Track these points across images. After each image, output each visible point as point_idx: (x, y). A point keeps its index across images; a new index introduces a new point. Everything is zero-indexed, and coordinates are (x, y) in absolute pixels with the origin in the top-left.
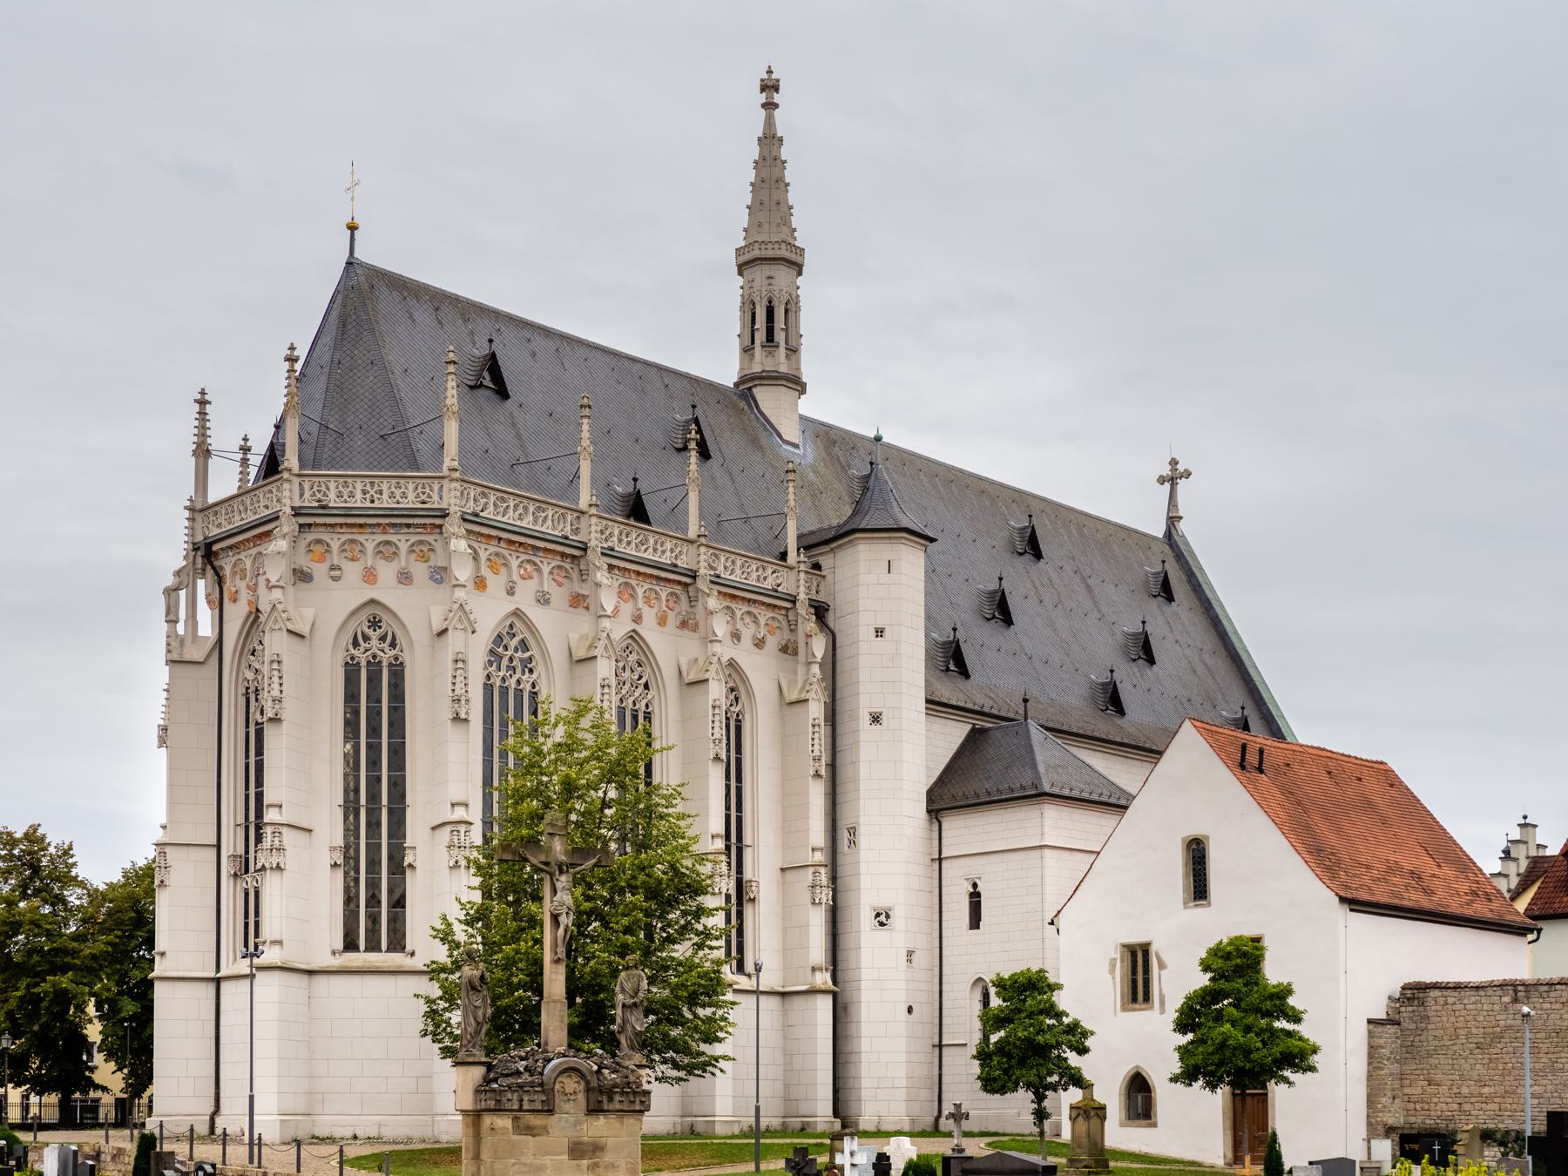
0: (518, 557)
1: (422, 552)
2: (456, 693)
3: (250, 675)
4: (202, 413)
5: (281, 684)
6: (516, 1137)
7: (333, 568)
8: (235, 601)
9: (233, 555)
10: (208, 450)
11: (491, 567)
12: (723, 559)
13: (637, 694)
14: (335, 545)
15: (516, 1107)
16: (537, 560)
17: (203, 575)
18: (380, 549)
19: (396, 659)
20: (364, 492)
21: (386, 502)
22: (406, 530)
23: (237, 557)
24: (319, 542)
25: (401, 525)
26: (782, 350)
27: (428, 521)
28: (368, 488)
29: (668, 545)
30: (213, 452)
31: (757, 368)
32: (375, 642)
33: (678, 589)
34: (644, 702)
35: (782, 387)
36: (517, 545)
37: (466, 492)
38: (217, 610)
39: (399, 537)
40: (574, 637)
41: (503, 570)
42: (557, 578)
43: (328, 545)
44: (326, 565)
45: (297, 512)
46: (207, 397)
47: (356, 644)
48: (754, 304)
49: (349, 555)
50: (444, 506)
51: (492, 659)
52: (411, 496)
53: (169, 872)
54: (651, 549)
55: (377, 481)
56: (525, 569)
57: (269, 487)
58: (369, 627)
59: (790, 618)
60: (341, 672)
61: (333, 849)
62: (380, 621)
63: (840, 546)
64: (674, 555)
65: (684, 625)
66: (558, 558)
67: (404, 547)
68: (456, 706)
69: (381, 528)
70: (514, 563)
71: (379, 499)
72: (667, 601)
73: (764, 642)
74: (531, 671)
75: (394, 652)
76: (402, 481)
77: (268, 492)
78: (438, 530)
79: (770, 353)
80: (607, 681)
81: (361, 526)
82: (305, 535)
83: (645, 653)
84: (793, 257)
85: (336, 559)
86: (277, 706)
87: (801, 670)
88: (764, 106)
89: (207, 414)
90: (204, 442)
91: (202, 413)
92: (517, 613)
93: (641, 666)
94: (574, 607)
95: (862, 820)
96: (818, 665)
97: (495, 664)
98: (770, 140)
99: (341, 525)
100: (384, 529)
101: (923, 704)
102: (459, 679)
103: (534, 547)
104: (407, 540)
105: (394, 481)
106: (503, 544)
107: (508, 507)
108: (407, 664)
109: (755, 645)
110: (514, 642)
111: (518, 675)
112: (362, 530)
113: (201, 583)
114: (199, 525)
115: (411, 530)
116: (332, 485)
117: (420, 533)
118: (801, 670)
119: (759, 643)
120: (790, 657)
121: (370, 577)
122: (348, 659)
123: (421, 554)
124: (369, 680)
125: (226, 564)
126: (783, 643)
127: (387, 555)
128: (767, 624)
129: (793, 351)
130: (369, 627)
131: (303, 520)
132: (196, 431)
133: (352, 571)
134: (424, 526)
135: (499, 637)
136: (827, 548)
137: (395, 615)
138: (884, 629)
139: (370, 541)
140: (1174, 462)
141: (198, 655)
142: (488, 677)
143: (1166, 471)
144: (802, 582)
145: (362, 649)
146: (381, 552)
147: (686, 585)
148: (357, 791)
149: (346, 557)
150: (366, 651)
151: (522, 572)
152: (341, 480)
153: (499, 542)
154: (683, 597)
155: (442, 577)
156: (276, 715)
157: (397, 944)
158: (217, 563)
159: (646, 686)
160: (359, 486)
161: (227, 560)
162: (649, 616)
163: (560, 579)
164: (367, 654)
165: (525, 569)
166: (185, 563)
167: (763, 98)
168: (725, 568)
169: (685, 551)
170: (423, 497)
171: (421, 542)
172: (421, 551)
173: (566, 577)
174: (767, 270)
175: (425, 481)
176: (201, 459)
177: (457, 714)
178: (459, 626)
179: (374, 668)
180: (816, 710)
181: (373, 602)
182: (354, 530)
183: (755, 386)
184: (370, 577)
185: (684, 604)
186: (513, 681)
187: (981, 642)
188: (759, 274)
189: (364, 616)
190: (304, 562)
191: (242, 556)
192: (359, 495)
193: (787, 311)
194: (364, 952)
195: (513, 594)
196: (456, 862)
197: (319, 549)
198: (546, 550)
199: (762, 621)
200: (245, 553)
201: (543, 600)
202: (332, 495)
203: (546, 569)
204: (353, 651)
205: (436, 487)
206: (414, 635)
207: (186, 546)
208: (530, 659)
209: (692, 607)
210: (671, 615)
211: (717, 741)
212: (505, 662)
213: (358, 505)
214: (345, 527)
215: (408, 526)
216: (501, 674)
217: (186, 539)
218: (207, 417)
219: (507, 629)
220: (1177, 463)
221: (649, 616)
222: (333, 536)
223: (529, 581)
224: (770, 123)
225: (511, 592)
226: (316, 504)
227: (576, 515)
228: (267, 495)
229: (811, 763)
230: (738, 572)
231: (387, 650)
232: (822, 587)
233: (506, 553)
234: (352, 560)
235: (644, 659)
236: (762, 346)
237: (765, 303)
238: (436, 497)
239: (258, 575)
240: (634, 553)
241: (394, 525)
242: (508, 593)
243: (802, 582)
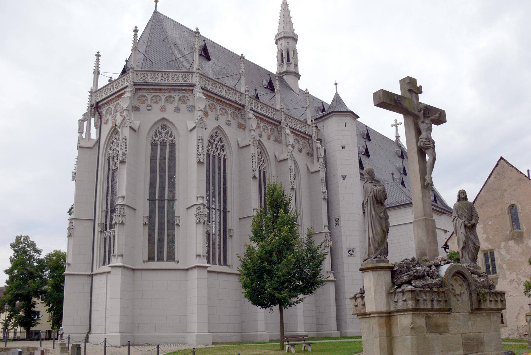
0: (220, 106)
2: (199, 152)
3: (110, 152)
4: (98, 60)
5: (126, 148)
6: (429, 335)
7: (148, 106)
8: (106, 123)
9: (107, 107)
10: (99, 72)
11: (210, 109)
12: (288, 119)
13: (261, 164)
14: (149, 97)
15: (429, 307)
16: (226, 108)
17: (94, 116)
18: (168, 99)
21: (171, 81)
22: (178, 92)
23: (108, 107)
24: (143, 96)
25: (176, 89)
26: (292, 66)
28: (163, 76)
29: (271, 111)
30: (101, 73)
31: (284, 69)
32: (163, 135)
33: (274, 127)
34: (263, 167)
35: (293, 76)
36: (220, 101)
37: (202, 79)
38: (99, 129)
40: (239, 139)
41: (214, 110)
42: (233, 116)
43: (146, 97)
44: (146, 105)
45: (135, 84)
46: (100, 54)
47: (156, 135)
48: (282, 51)
50: (194, 82)
51: (210, 144)
52: (180, 79)
54: (265, 111)
55: (167, 73)
56: (222, 112)
57: (124, 77)
58: (162, 129)
59: (310, 143)
60: (149, 147)
62: (166, 127)
63: (326, 119)
64: (273, 114)
65: (276, 140)
66: (234, 109)
68: (199, 157)
69: (168, 91)
70: (218, 108)
71: (168, 80)
72: (270, 131)
73: (302, 151)
74: (223, 151)
75: (171, 139)
76: (177, 74)
77: (123, 79)
78: (191, 92)
79: (289, 65)
80: (254, 154)
81: (160, 90)
82: (138, 93)
83: (264, 150)
84: (295, 37)
85: (149, 103)
86: (124, 156)
87: (316, 160)
89: (99, 60)
90: (97, 69)
91: (98, 60)
92: (219, 128)
93: (261, 154)
94: (239, 128)
96: (322, 159)
97: (210, 146)
99: (152, 89)
100: (170, 91)
101: (359, 175)
102: (200, 147)
103: (225, 103)
104: (178, 96)
105: (174, 74)
106: (214, 101)
107: (217, 87)
108: (177, 143)
109: (299, 151)
110: (218, 139)
111: (219, 151)
112: (160, 92)
113: (93, 119)
114: (94, 98)
115: (180, 92)
116: (149, 75)
117: (184, 93)
118: (316, 160)
119: (300, 151)
120: (309, 157)
121: (163, 109)
122: (153, 141)
123: (184, 101)
124: (161, 149)
125: (104, 111)
126: (308, 151)
127: (170, 101)
128: (302, 144)
129: (296, 65)
130: (162, 129)
131: (137, 87)
132: (95, 65)
134: (185, 90)
135: (212, 136)
136: (320, 120)
137: (173, 124)
138: (345, 146)
139: (163, 96)
140: (396, 120)
141: (91, 145)
142: (208, 151)
143: (394, 123)
144: (314, 130)
145: (158, 137)
146: (168, 100)
147: (277, 126)
148: (155, 194)
149: (153, 102)
150: (160, 138)
151: (221, 112)
152: (153, 73)
153: (213, 100)
154: (276, 130)
155: (192, 110)
156: (124, 160)
158: (100, 111)
159: (263, 162)
161: (104, 109)
162: (265, 136)
163: (234, 117)
164: (160, 139)
165: (222, 112)
166: (87, 111)
168: (289, 122)
169: (276, 113)
170: (185, 79)
171: (184, 96)
172: (184, 100)
173: (236, 117)
174: (287, 40)
176: (96, 75)
177: (200, 160)
178: (200, 126)
179: (163, 144)
180: (322, 175)
181: (164, 119)
183: (284, 75)
185: (276, 133)
186: (217, 153)
187: (364, 159)
188: (283, 42)
190: (135, 103)
191: (110, 106)
192: (160, 78)
193: (293, 53)
194: (157, 261)
195: (217, 120)
196: (200, 221)
197: (143, 99)
198: (230, 105)
199: (301, 143)
200: (111, 105)
201: (228, 124)
202: (149, 78)
203: (229, 112)
204: (155, 138)
205: (190, 76)
207: (88, 105)
208: (223, 146)
209: (279, 134)
210: (272, 136)
211: (292, 182)
212: (214, 146)
213: (160, 82)
214: (154, 90)
215: (179, 90)
216: (213, 150)
217: (88, 103)
218: (99, 61)
219: (215, 133)
220: (397, 120)
221: (265, 136)
222: (149, 94)
223: (223, 116)
225: (217, 119)
226: (143, 82)
227: (240, 94)
228: (123, 81)
229: (322, 194)
230: (293, 124)
231: (168, 138)
232: (319, 134)
233: (216, 104)
235: (263, 152)
236: (286, 63)
237: (286, 50)
239: (117, 112)
240: (259, 111)
241: (173, 89)
242: (216, 119)
243: (314, 130)
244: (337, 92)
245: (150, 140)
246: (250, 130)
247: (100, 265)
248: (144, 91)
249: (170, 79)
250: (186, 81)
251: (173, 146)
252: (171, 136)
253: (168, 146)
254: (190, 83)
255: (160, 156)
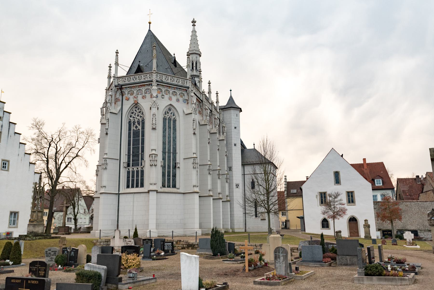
1: (182, 95)
3: (132, 119)
14: (163, 90)
19: (174, 118)
20: (170, 79)
27: (185, 88)
30: (119, 65)
32: (170, 114)
39: (177, 91)
43: (162, 90)
47: (165, 114)
49: (166, 93)
50: (188, 85)
52: (181, 82)
53: (107, 165)
55: (173, 77)
61: (161, 162)
67: (178, 93)
68: (194, 131)
81: (170, 87)
88: (193, 25)
95: (233, 165)
98: (194, 32)
99: (165, 86)
115: (180, 90)
116: (164, 77)
121: (170, 99)
133: (166, 97)
134: (183, 89)
137: (175, 108)
139: (171, 91)
145: (167, 115)
148: (165, 148)
150: (168, 116)
152: (166, 76)
157: (174, 186)
158: (122, 91)
160: (170, 78)
167: (192, 24)
170: (183, 83)
171: (182, 93)
175: (184, 79)
181: (171, 105)
182: (168, 88)
184: (170, 99)
189: (168, 108)
202: (164, 78)
205: (186, 82)
206: (180, 114)
215: (180, 89)
224: (194, 29)
226: (160, 80)
228: (145, 76)
234: (166, 94)
238: (186, 84)
244: (231, 95)
245: (163, 116)
246: (207, 116)
247: (125, 189)
248: (161, 86)
249: (175, 81)
250: (183, 84)
251: (175, 121)
252: (174, 115)
253: (172, 121)
254: (186, 85)
255: (168, 126)
